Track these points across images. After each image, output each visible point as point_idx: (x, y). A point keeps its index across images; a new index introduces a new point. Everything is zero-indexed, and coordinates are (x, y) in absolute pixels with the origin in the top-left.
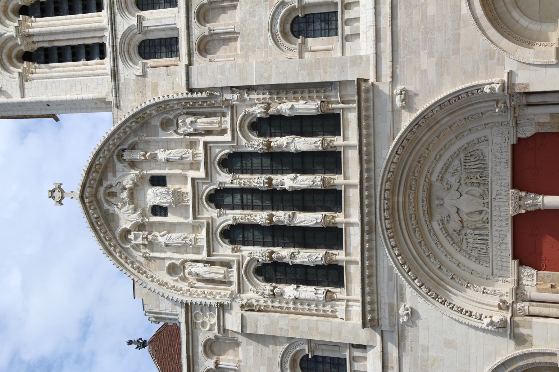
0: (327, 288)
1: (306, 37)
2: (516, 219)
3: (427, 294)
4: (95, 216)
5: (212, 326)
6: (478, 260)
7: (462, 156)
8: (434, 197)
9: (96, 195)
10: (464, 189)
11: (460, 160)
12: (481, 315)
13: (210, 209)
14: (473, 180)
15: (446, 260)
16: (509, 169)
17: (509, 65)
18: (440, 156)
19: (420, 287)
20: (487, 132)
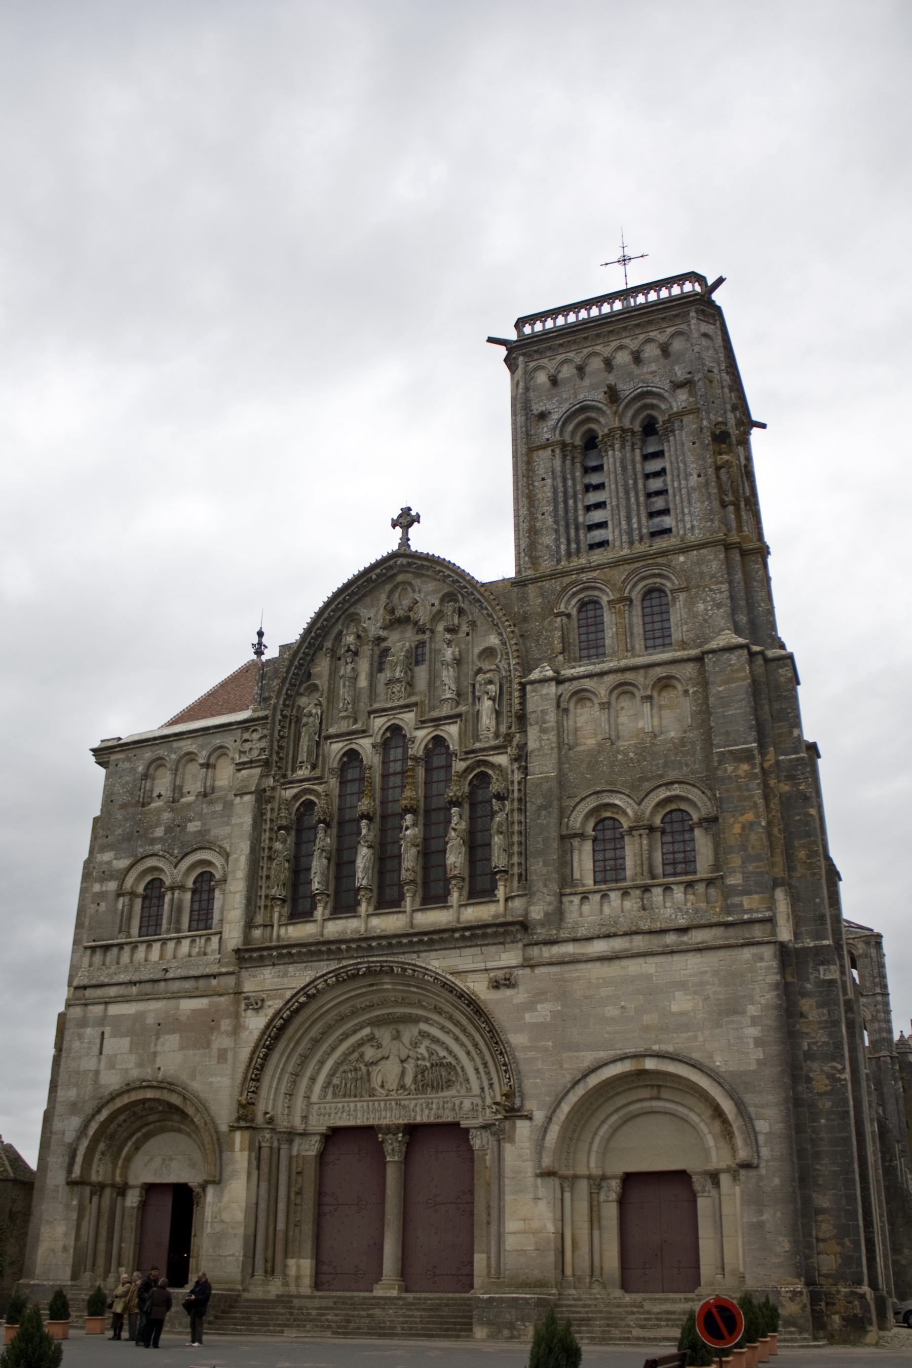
0: (289, 899)
1: (595, 840)
2: (368, 1131)
3: (274, 1027)
4: (374, 577)
5: (242, 752)
6: (328, 1084)
7: (450, 1059)
8: (401, 1027)
9: (403, 569)
10: (410, 1067)
11: (444, 1057)
12: (253, 1092)
13: (382, 731)
14: (419, 1076)
15: (325, 1047)
16: (432, 1120)
17: (539, 1116)
18: (448, 1033)
19: (282, 1018)
20: (476, 1090)
